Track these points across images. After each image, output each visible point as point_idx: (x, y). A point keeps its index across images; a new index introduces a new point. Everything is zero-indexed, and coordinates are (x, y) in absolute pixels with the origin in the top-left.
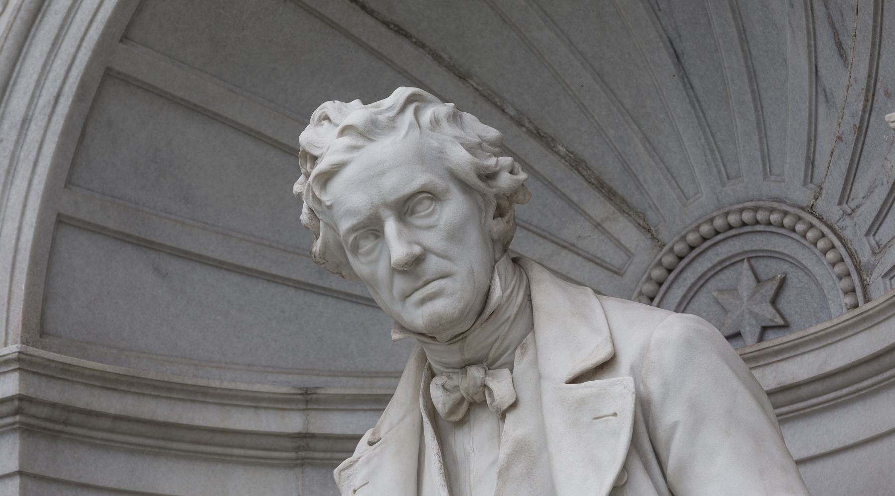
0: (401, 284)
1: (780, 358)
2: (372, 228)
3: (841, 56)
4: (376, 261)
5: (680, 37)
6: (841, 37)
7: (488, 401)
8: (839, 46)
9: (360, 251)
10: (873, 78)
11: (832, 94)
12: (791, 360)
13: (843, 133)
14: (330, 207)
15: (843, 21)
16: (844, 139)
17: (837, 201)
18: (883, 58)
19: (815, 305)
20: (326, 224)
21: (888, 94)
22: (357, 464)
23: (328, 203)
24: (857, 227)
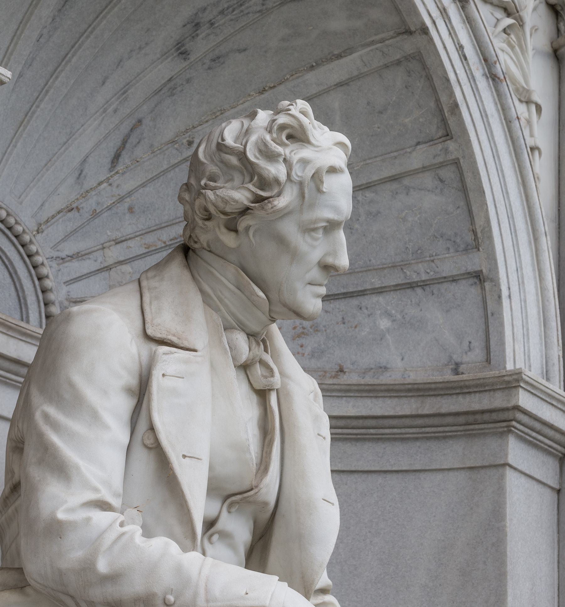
0: (315, 274)
1: (24, 339)
2: (331, 226)
3: (113, 162)
4: (314, 247)
5: (30, 65)
6: (124, 153)
7: (258, 370)
8: (117, 157)
9: (313, 234)
10: (130, 194)
11: (85, 177)
12: (29, 345)
13: (83, 208)
14: (319, 191)
15: (135, 146)
16: (81, 211)
17: (52, 245)
18: (147, 189)
19: (11, 304)
20: (302, 195)
21: (131, 210)
22: (172, 356)
23: (324, 190)
24: (60, 273)
